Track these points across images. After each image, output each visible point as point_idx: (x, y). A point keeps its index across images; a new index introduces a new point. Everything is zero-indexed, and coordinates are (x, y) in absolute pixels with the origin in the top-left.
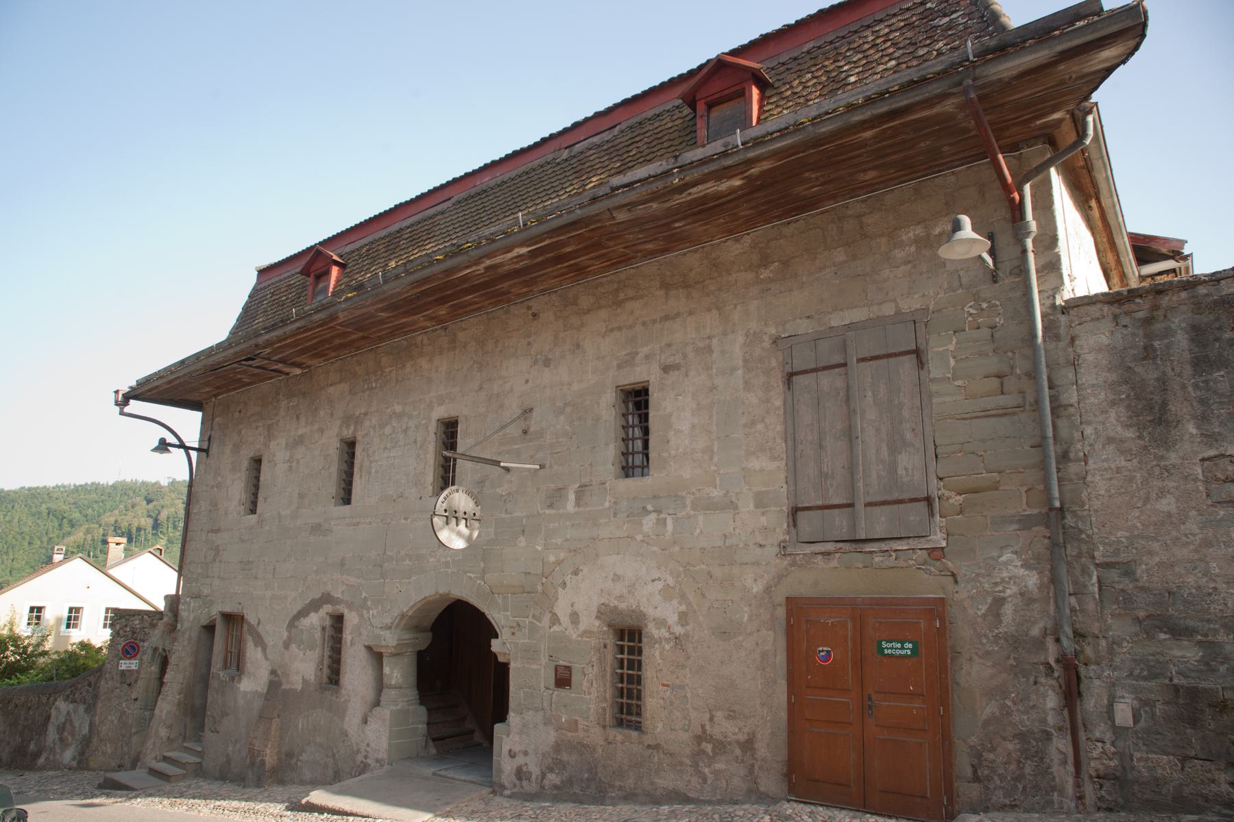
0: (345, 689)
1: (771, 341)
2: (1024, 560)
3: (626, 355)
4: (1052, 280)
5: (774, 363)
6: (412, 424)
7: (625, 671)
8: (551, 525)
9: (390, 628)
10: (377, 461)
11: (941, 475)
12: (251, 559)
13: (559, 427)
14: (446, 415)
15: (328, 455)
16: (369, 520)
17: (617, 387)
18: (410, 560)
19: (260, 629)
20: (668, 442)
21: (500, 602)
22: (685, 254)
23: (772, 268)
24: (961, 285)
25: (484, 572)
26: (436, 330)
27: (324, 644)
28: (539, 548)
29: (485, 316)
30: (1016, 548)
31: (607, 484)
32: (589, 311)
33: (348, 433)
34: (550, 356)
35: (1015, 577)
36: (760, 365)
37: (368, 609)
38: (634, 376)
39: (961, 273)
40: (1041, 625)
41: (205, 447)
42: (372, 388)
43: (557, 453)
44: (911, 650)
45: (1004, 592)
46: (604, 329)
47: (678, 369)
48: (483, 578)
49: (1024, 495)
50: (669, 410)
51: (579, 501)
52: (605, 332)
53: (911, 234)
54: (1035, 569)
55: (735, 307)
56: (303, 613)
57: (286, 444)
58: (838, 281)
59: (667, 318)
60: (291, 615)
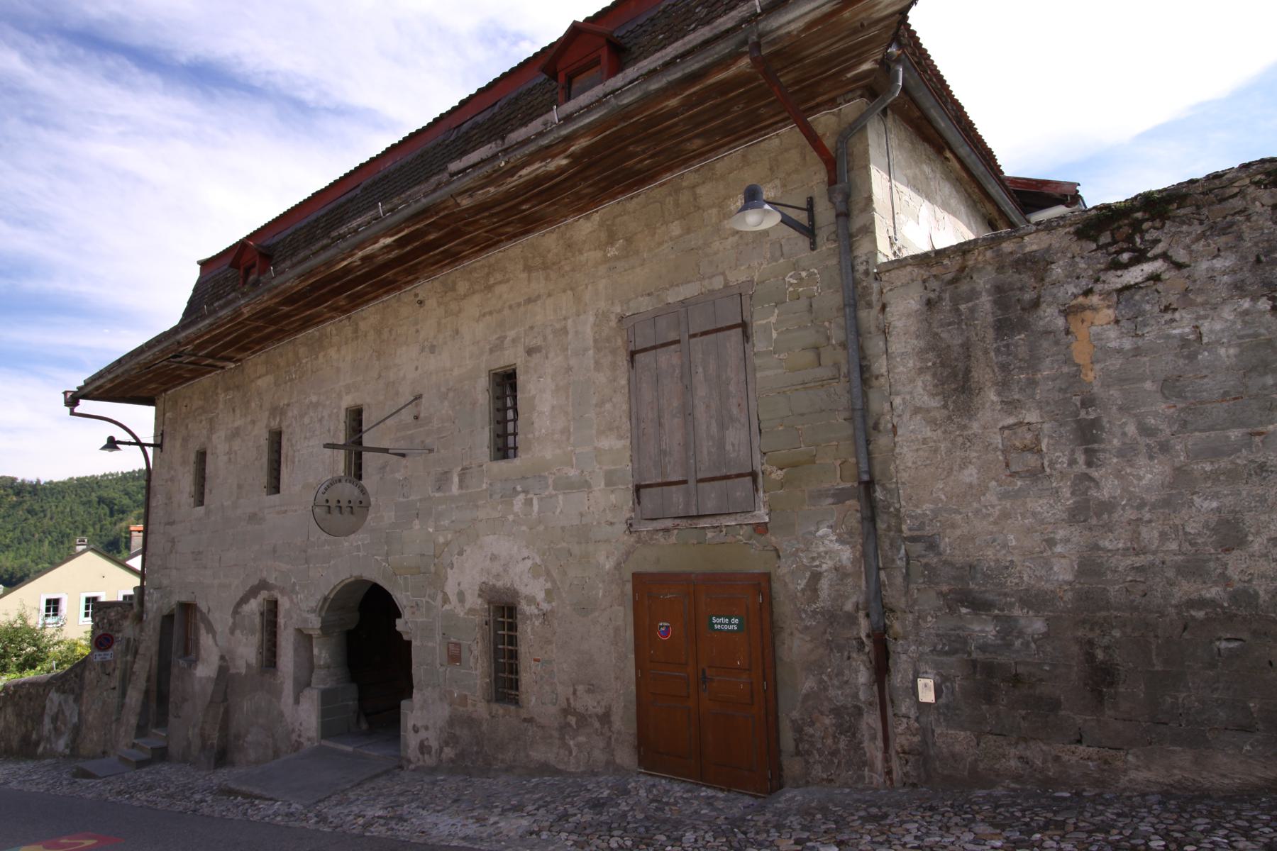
3: (497, 339)
5: (619, 342)
7: (506, 647)
10: (299, 451)
11: (765, 451)
14: (352, 404)
19: (211, 617)
24: (782, 255)
25: (387, 554)
28: (431, 530)
30: (831, 522)
32: (465, 296)
33: (274, 424)
34: (435, 343)
37: (297, 593)
38: (503, 360)
39: (783, 242)
40: (854, 599)
41: (159, 442)
43: (443, 437)
44: (737, 625)
47: (540, 352)
49: (838, 468)
50: (533, 392)
54: (848, 543)
56: (244, 600)
57: (226, 437)
59: (529, 301)
60: (234, 603)
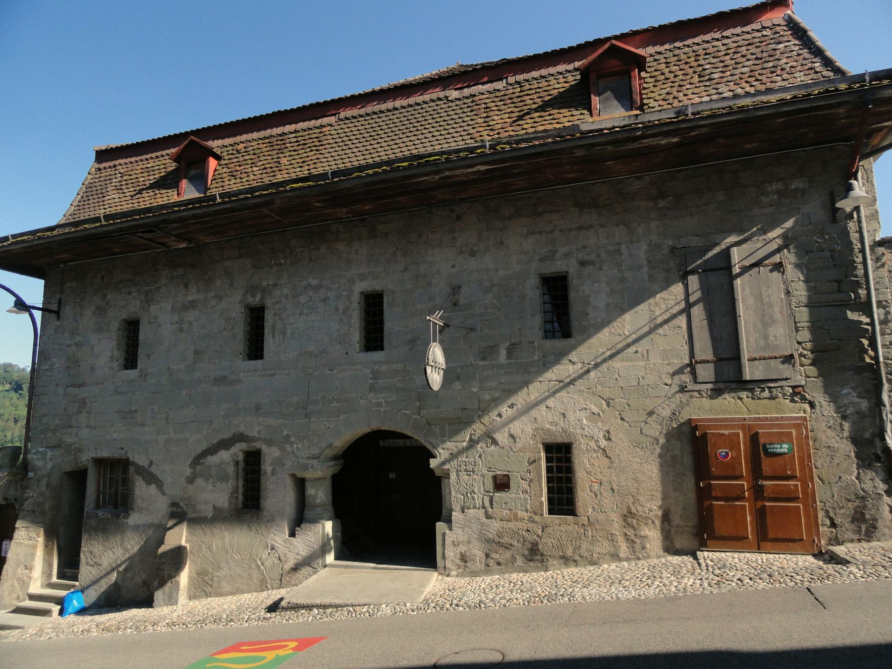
0: (268, 511)
1: (669, 250)
2: (858, 393)
3: (546, 252)
4: (874, 224)
5: (672, 264)
6: (331, 295)
7: (555, 474)
8: (485, 373)
9: (318, 458)
10: (292, 324)
11: (800, 341)
12: (133, 408)
13: (487, 301)
14: (369, 289)
15: (230, 319)
16: (287, 371)
17: (540, 274)
18: (337, 402)
19: (153, 469)
20: (587, 314)
21: (438, 431)
22: (594, 184)
23: (668, 200)
24: (811, 223)
25: (420, 409)
26: (353, 221)
27: (237, 476)
28: (475, 390)
29: (406, 214)
30: (853, 385)
31: (536, 344)
32: (510, 218)
33: (255, 300)
34: (475, 249)
35: (852, 403)
36: (661, 265)
37: (291, 444)
38: (557, 266)
39: (811, 215)
40: (871, 430)
41: (54, 307)
42: (281, 264)
43: (487, 320)
44: (788, 449)
45: (846, 412)
46: (525, 232)
47: (594, 265)
48: (419, 414)
49: (857, 354)
50: (587, 292)
51: (510, 355)
52: (527, 234)
53: (774, 187)
54: (866, 398)
55: (639, 224)
56: (212, 450)
57: (173, 308)
58: (719, 214)
59: (581, 228)
60: (194, 455)
